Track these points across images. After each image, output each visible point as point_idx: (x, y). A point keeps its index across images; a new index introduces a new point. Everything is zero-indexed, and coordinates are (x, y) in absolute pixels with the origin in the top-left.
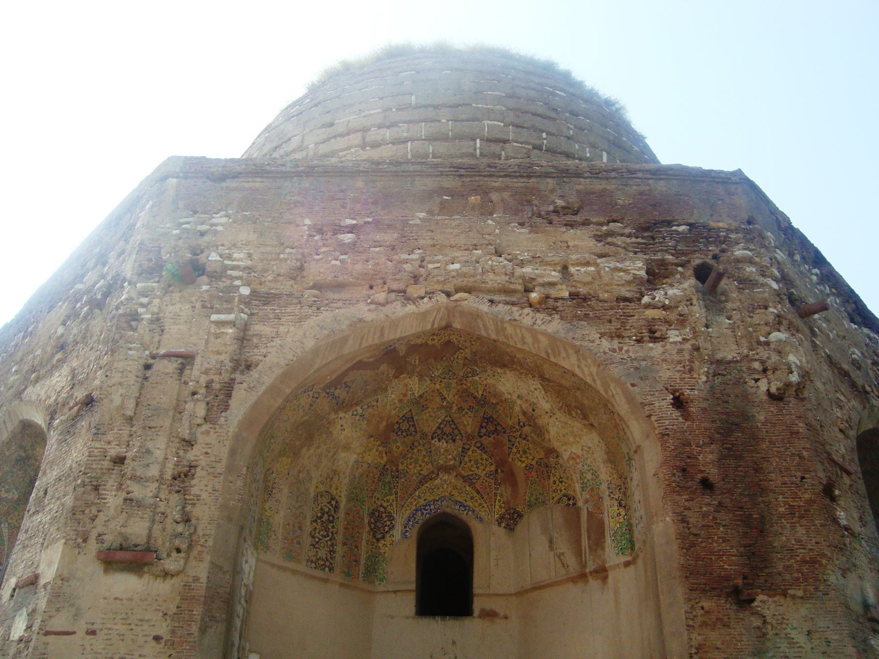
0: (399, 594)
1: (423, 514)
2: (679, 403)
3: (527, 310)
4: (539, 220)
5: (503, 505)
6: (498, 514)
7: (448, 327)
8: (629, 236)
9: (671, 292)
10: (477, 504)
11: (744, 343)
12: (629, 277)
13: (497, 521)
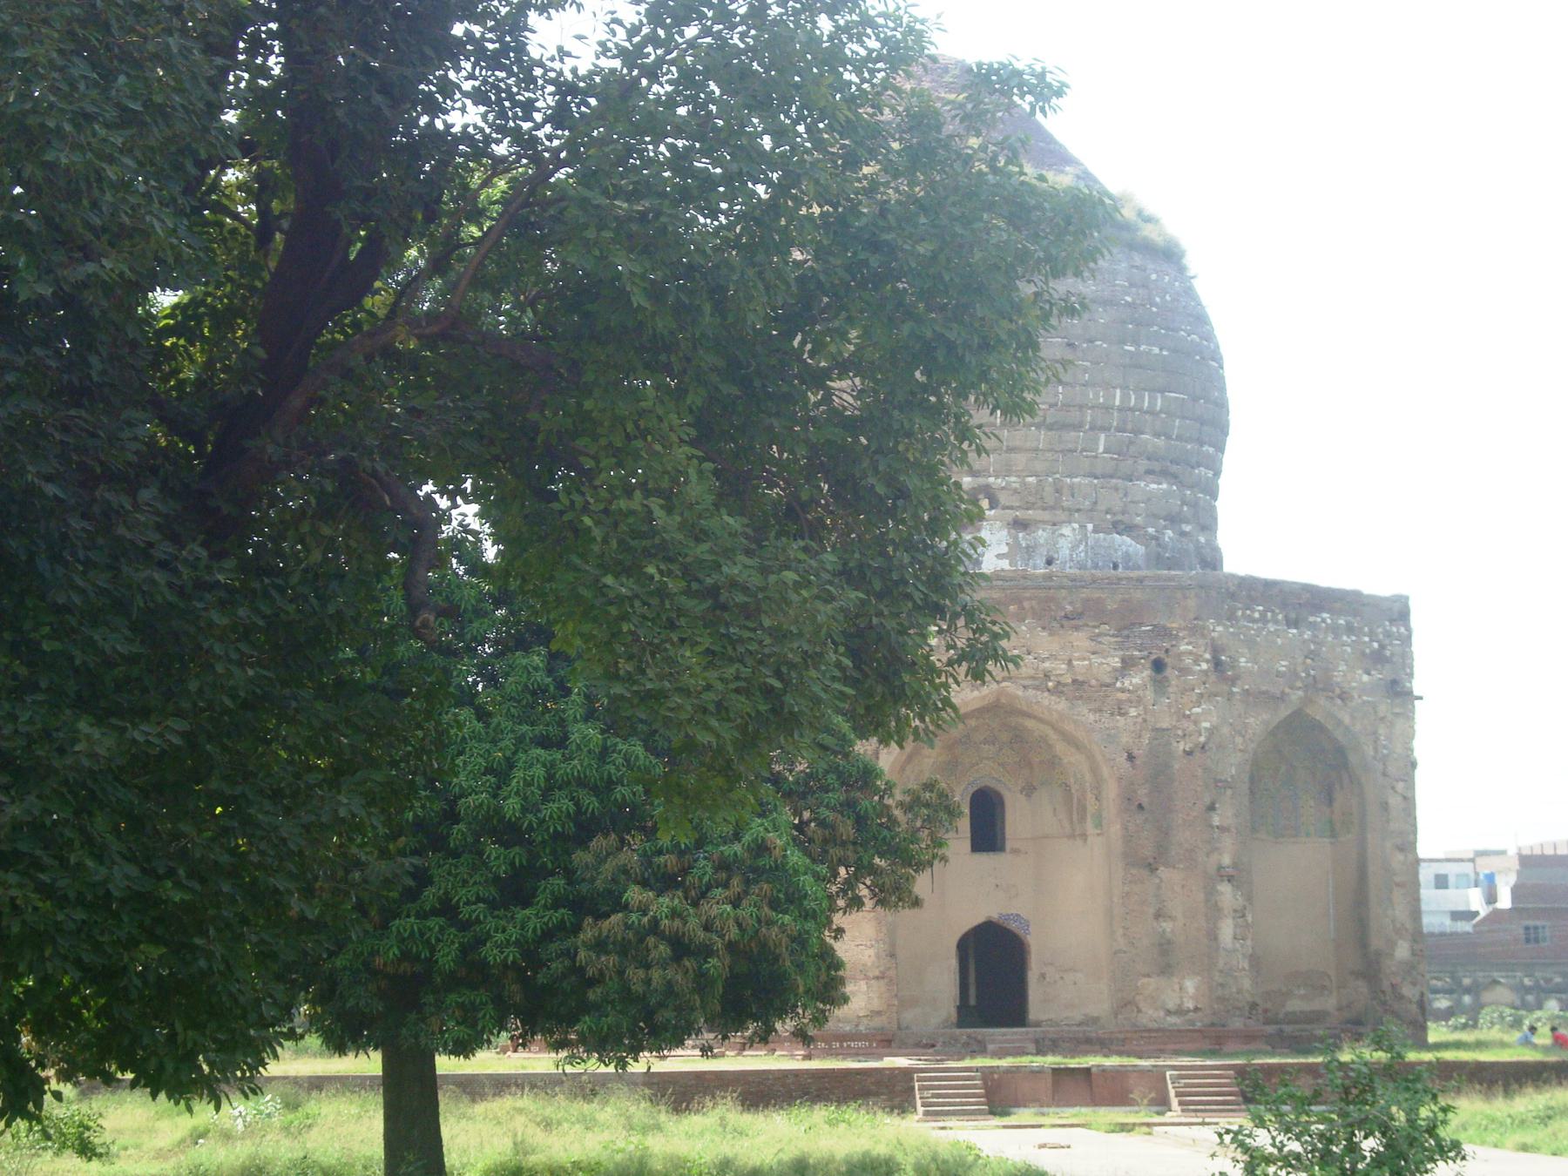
2: (1131, 757)
3: (1046, 694)
4: (1054, 624)
7: (998, 700)
8: (1113, 636)
9: (1134, 681)
11: (1175, 718)
12: (1109, 669)
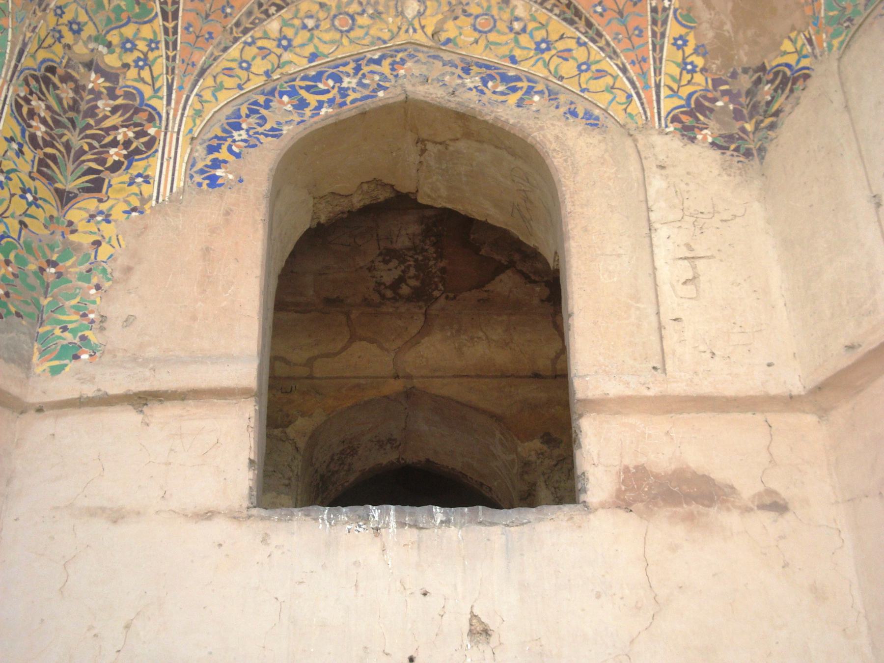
0: (159, 413)
1: (302, 104)
5: (699, 62)
6: (675, 93)
10: (568, 68)
13: (675, 119)
